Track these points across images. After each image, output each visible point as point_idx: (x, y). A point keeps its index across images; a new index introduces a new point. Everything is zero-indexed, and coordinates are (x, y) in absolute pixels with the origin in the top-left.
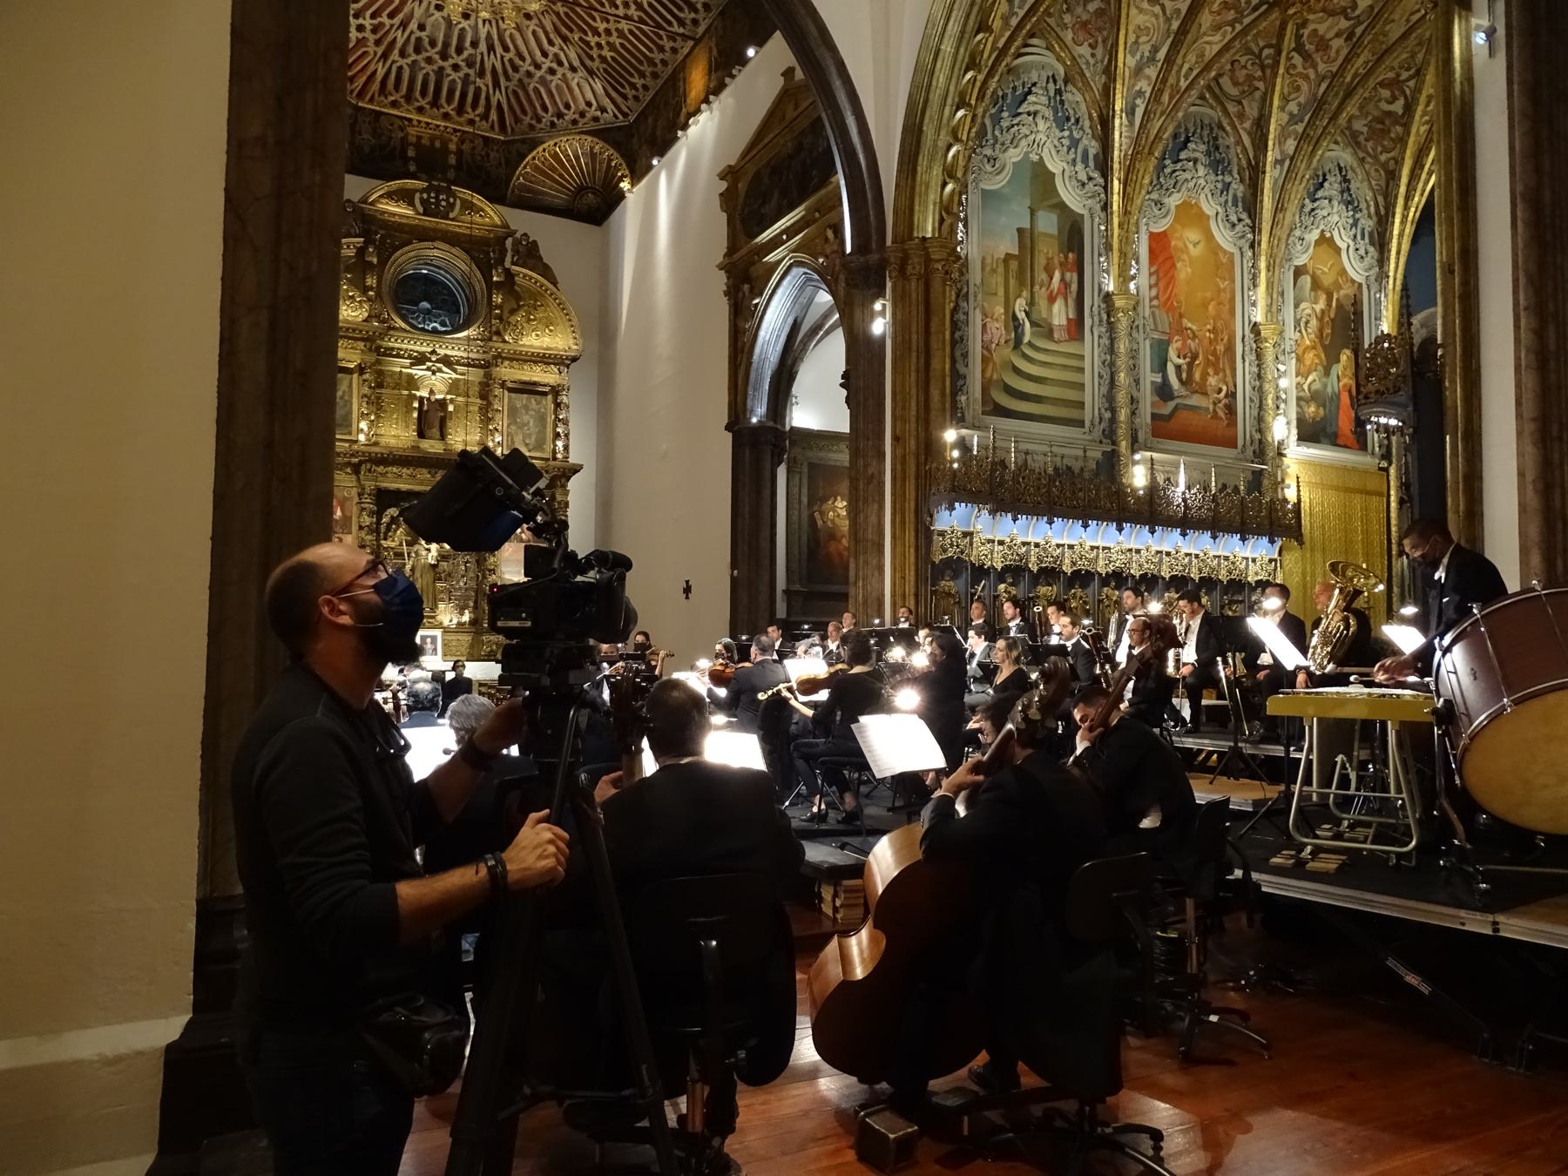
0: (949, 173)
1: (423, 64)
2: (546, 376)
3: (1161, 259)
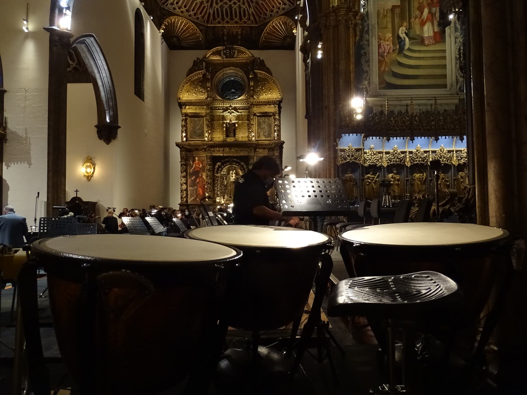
2: (271, 109)
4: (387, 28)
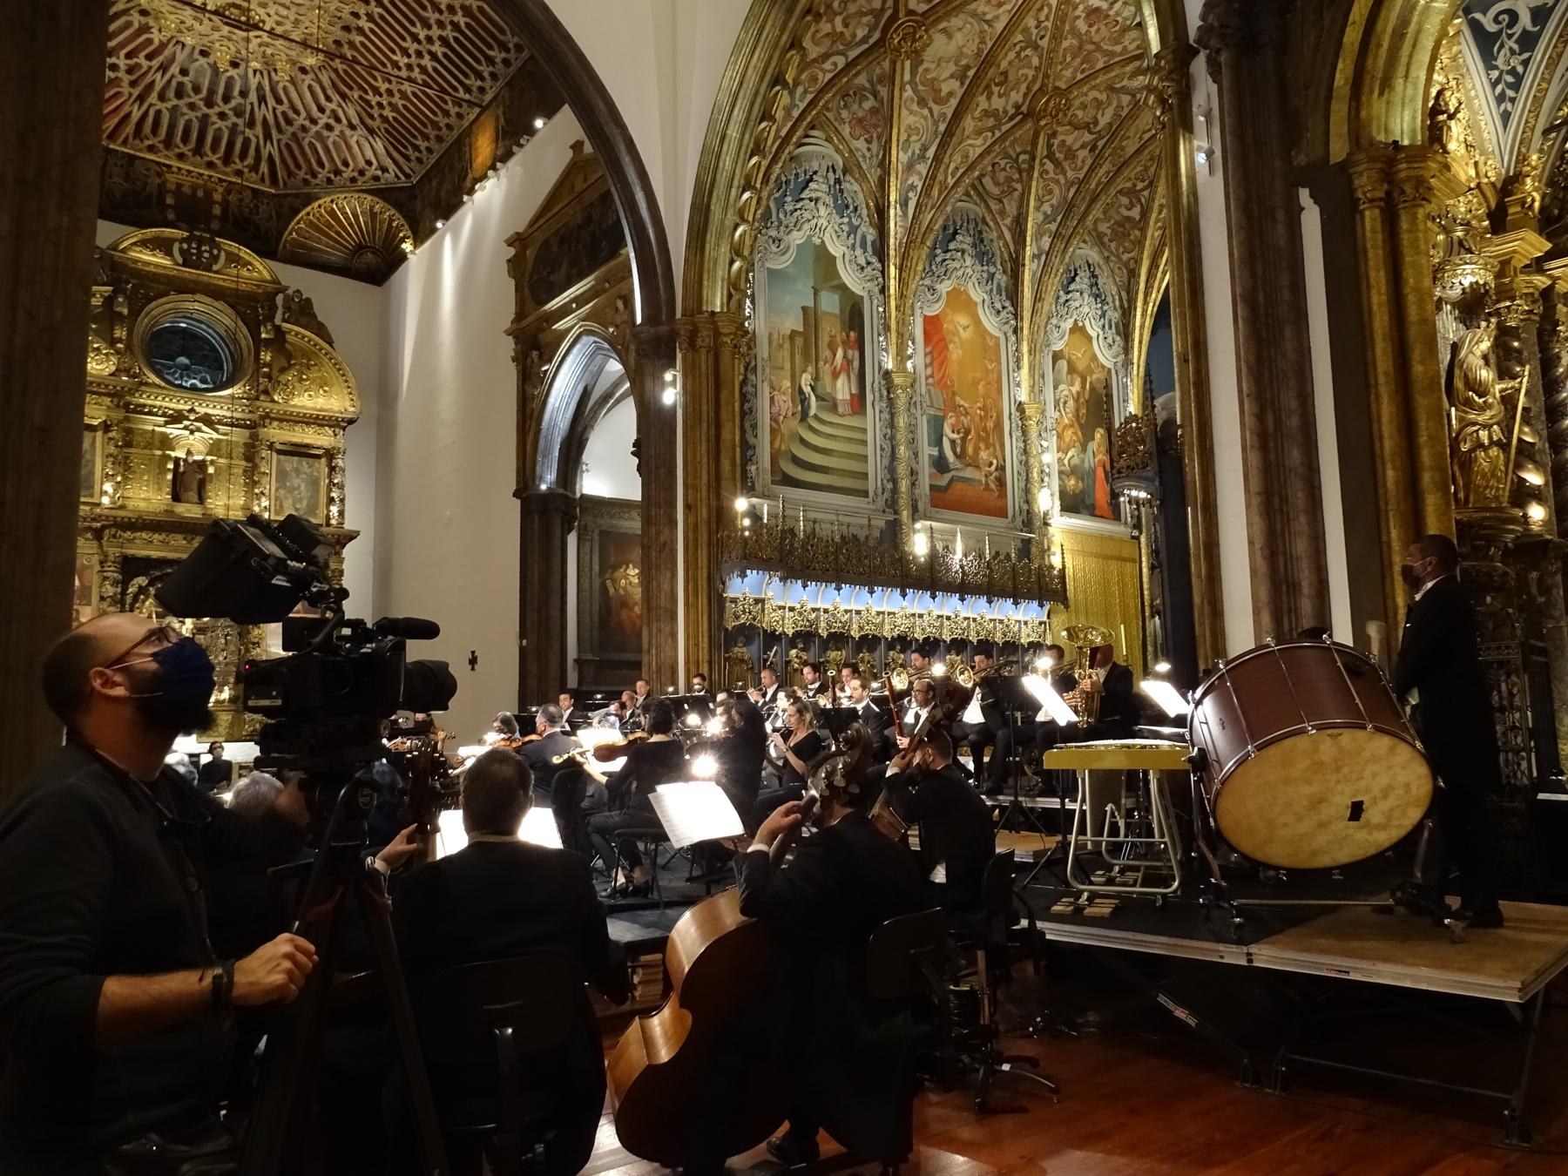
0: (737, 251)
1: (185, 110)
2: (320, 438)
3: (935, 340)
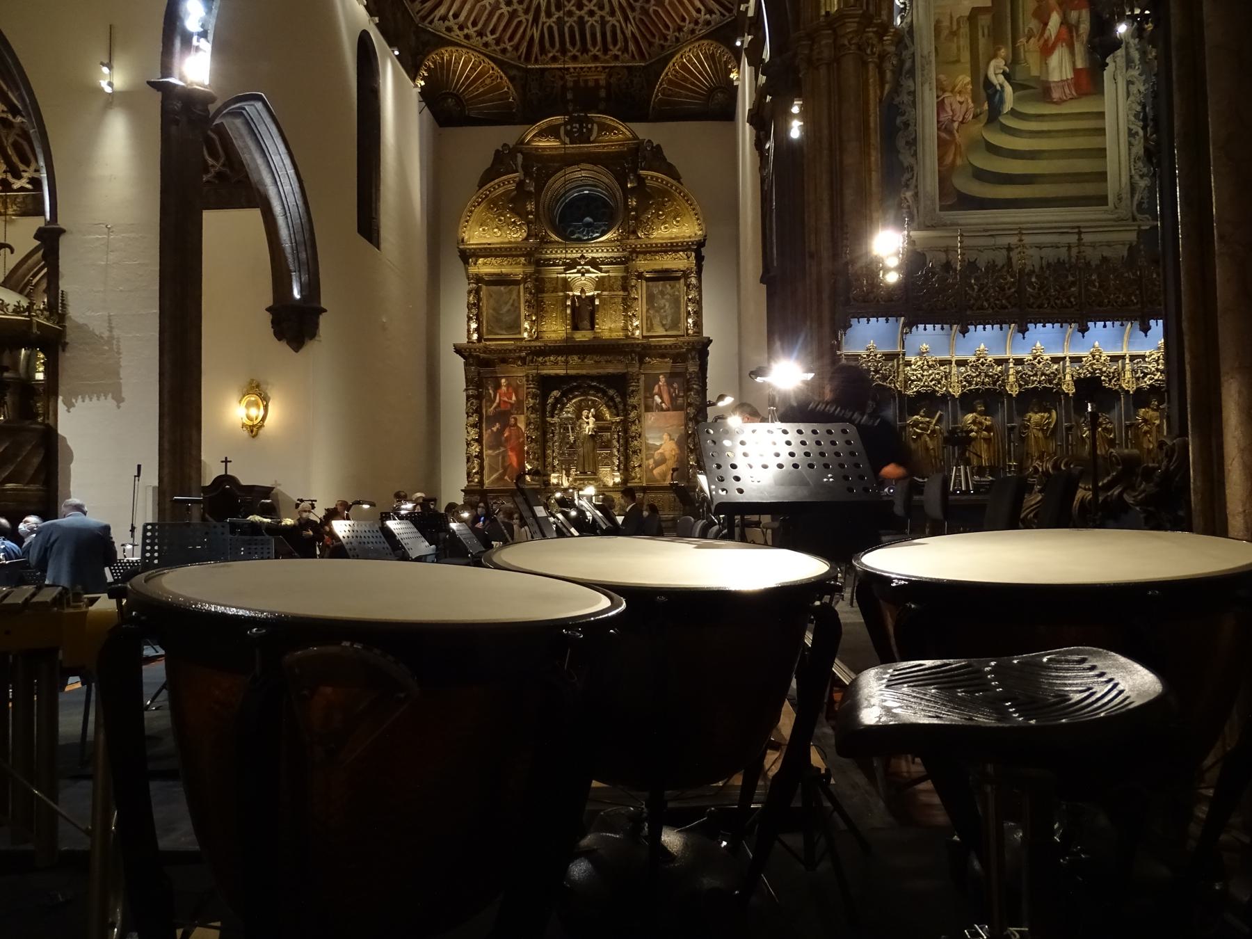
4: (958, 61)
